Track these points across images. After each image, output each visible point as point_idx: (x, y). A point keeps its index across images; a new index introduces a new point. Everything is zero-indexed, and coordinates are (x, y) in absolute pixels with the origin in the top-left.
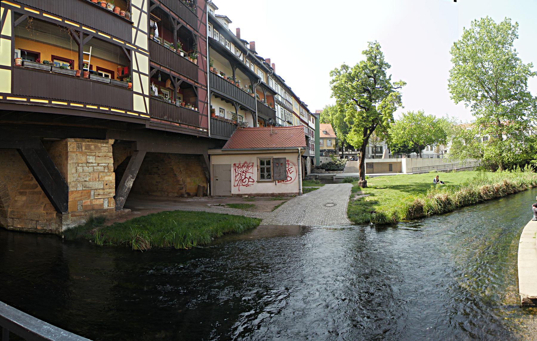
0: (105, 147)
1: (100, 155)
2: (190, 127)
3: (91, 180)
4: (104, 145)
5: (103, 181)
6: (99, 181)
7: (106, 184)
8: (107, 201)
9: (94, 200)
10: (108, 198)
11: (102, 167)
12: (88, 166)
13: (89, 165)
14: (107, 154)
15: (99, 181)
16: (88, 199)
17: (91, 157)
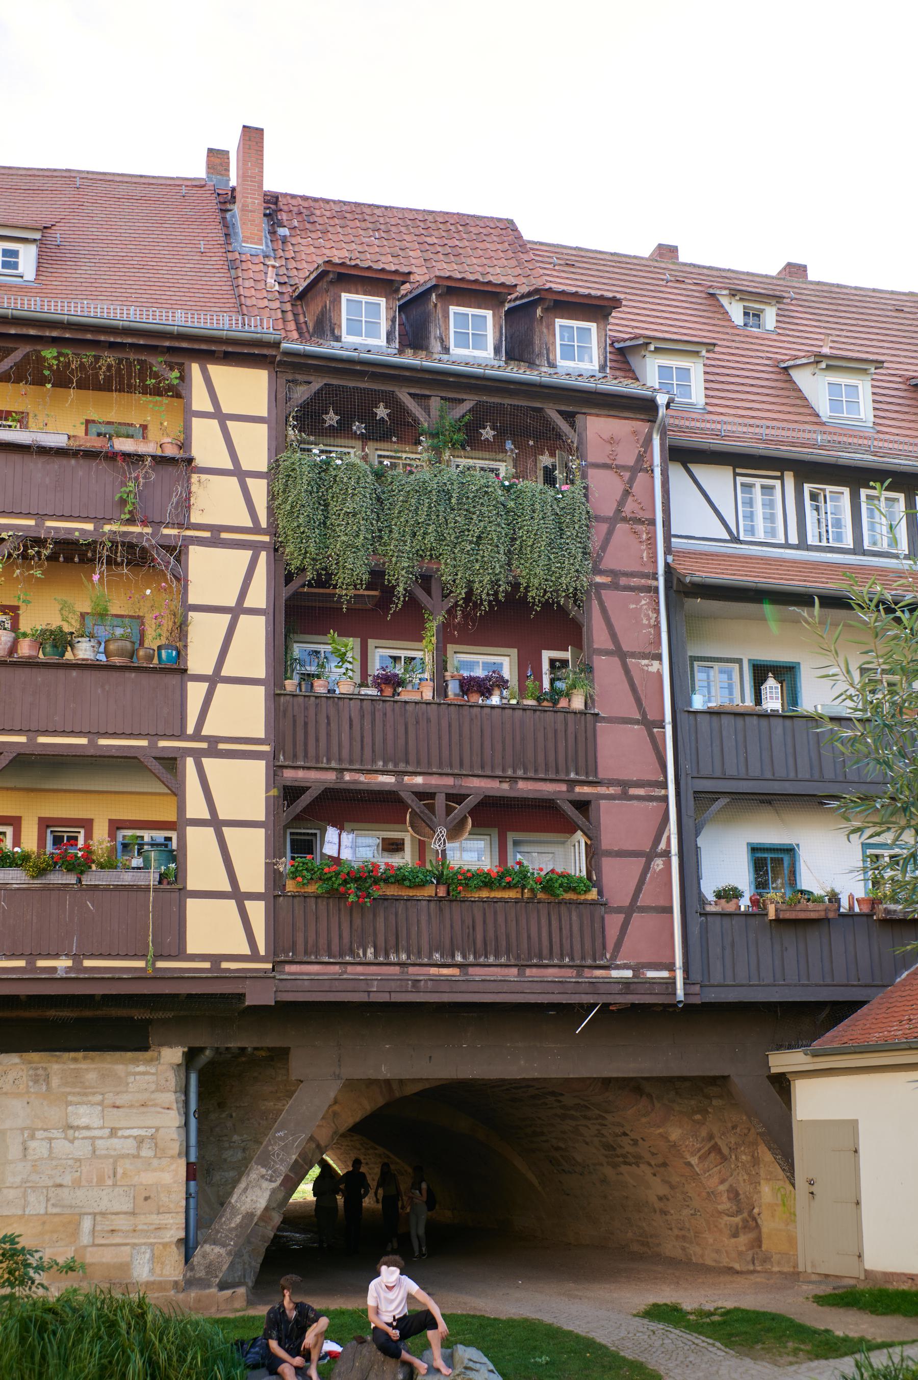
0: (144, 1073)
2: (528, 972)
3: (84, 1183)
4: (141, 1068)
6: (115, 1185)
7: (146, 1199)
8: (148, 1256)
9: (90, 1249)
10: (152, 1245)
11: (131, 1140)
12: (71, 1138)
14: (153, 1096)
15: (115, 1185)
17: (82, 1109)
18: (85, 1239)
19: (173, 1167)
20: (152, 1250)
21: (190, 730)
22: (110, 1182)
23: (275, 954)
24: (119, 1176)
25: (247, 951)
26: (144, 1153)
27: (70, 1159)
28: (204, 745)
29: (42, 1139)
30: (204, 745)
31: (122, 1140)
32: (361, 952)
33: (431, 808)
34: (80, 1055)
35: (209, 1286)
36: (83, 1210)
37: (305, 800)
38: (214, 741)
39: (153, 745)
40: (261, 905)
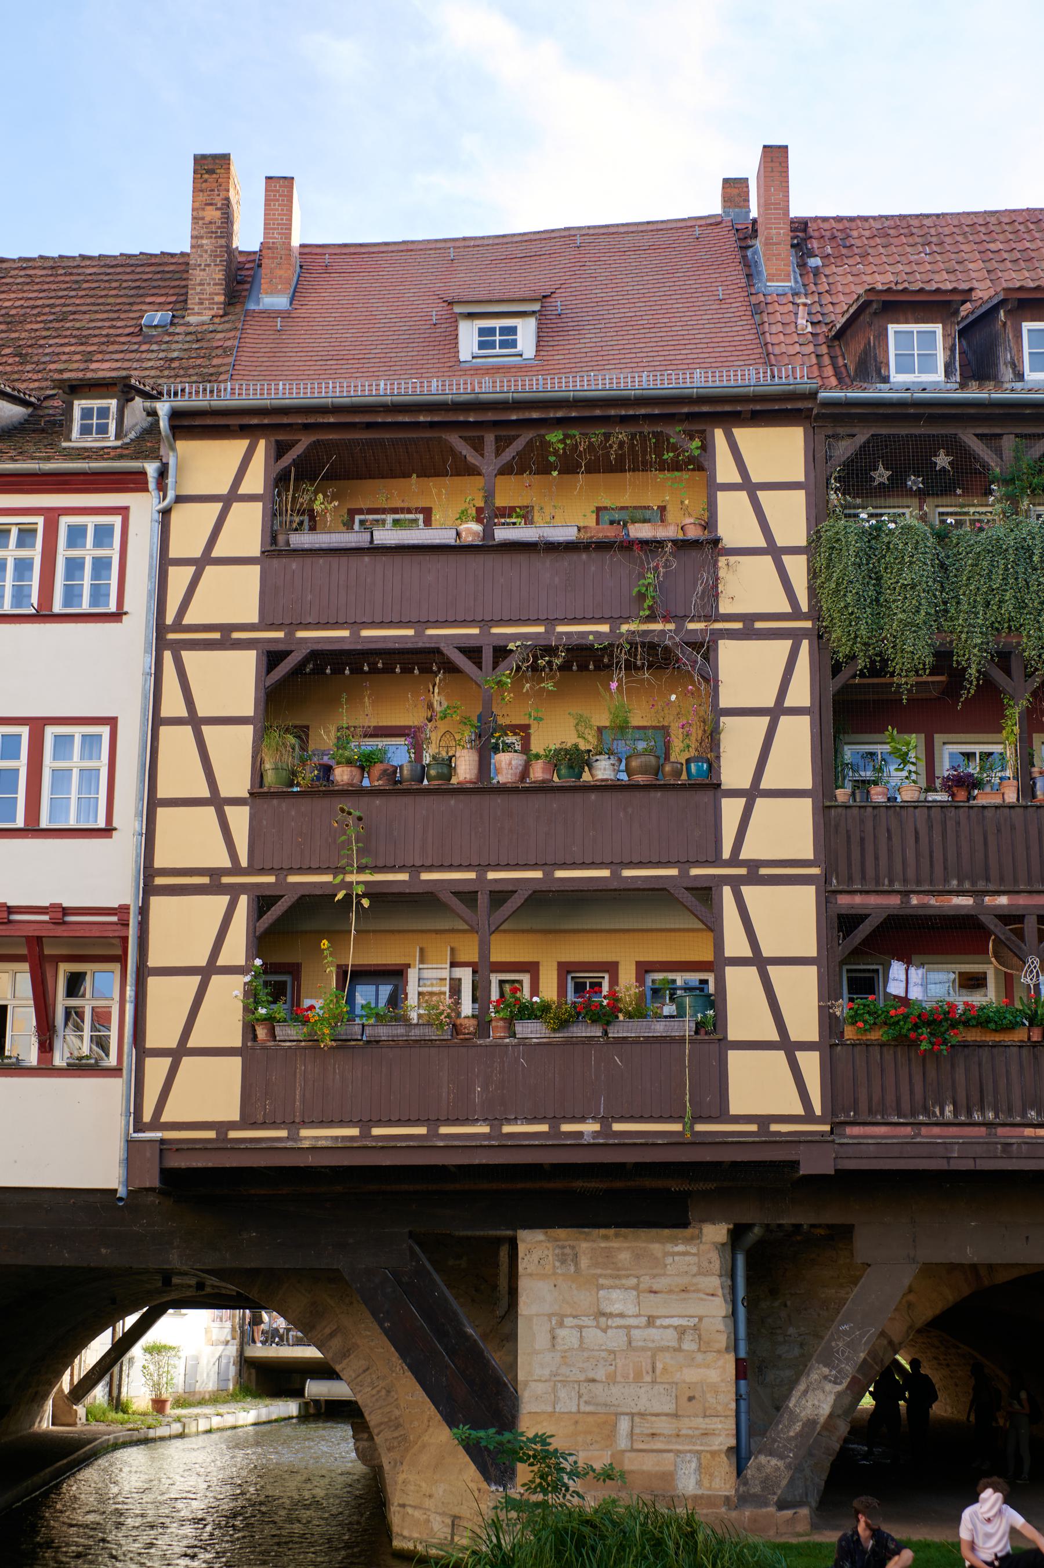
1: (659, 1284)
3: (619, 1378)
4: (680, 1248)
5: (677, 1384)
7: (691, 1399)
8: (694, 1465)
9: (628, 1454)
10: (698, 1452)
11: (671, 1331)
12: (604, 1326)
13: (610, 1322)
14: (695, 1280)
16: (602, 1450)
17: (615, 1294)
18: (623, 1443)
19: (720, 1363)
20: (699, 1459)
21: (726, 854)
22: (648, 1379)
23: (834, 1114)
24: (658, 1371)
25: (799, 1110)
26: (686, 1346)
27: (603, 1350)
28: (743, 871)
29: (572, 1327)
30: (743, 871)
31: (661, 1330)
32: (937, 1110)
33: (1020, 934)
34: (611, 1232)
35: (766, 1504)
36: (620, 1410)
37: (864, 930)
38: (754, 865)
39: (684, 874)
40: (815, 1056)
